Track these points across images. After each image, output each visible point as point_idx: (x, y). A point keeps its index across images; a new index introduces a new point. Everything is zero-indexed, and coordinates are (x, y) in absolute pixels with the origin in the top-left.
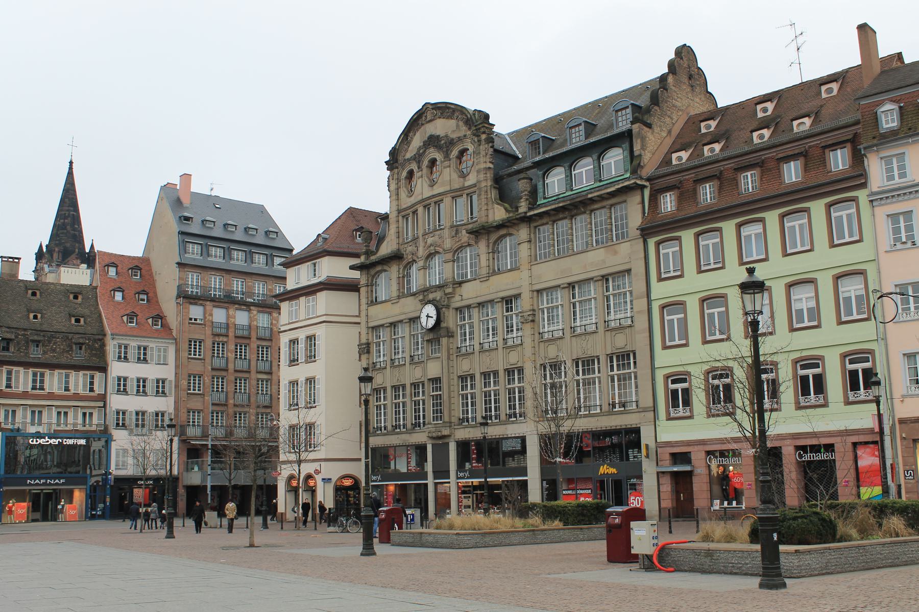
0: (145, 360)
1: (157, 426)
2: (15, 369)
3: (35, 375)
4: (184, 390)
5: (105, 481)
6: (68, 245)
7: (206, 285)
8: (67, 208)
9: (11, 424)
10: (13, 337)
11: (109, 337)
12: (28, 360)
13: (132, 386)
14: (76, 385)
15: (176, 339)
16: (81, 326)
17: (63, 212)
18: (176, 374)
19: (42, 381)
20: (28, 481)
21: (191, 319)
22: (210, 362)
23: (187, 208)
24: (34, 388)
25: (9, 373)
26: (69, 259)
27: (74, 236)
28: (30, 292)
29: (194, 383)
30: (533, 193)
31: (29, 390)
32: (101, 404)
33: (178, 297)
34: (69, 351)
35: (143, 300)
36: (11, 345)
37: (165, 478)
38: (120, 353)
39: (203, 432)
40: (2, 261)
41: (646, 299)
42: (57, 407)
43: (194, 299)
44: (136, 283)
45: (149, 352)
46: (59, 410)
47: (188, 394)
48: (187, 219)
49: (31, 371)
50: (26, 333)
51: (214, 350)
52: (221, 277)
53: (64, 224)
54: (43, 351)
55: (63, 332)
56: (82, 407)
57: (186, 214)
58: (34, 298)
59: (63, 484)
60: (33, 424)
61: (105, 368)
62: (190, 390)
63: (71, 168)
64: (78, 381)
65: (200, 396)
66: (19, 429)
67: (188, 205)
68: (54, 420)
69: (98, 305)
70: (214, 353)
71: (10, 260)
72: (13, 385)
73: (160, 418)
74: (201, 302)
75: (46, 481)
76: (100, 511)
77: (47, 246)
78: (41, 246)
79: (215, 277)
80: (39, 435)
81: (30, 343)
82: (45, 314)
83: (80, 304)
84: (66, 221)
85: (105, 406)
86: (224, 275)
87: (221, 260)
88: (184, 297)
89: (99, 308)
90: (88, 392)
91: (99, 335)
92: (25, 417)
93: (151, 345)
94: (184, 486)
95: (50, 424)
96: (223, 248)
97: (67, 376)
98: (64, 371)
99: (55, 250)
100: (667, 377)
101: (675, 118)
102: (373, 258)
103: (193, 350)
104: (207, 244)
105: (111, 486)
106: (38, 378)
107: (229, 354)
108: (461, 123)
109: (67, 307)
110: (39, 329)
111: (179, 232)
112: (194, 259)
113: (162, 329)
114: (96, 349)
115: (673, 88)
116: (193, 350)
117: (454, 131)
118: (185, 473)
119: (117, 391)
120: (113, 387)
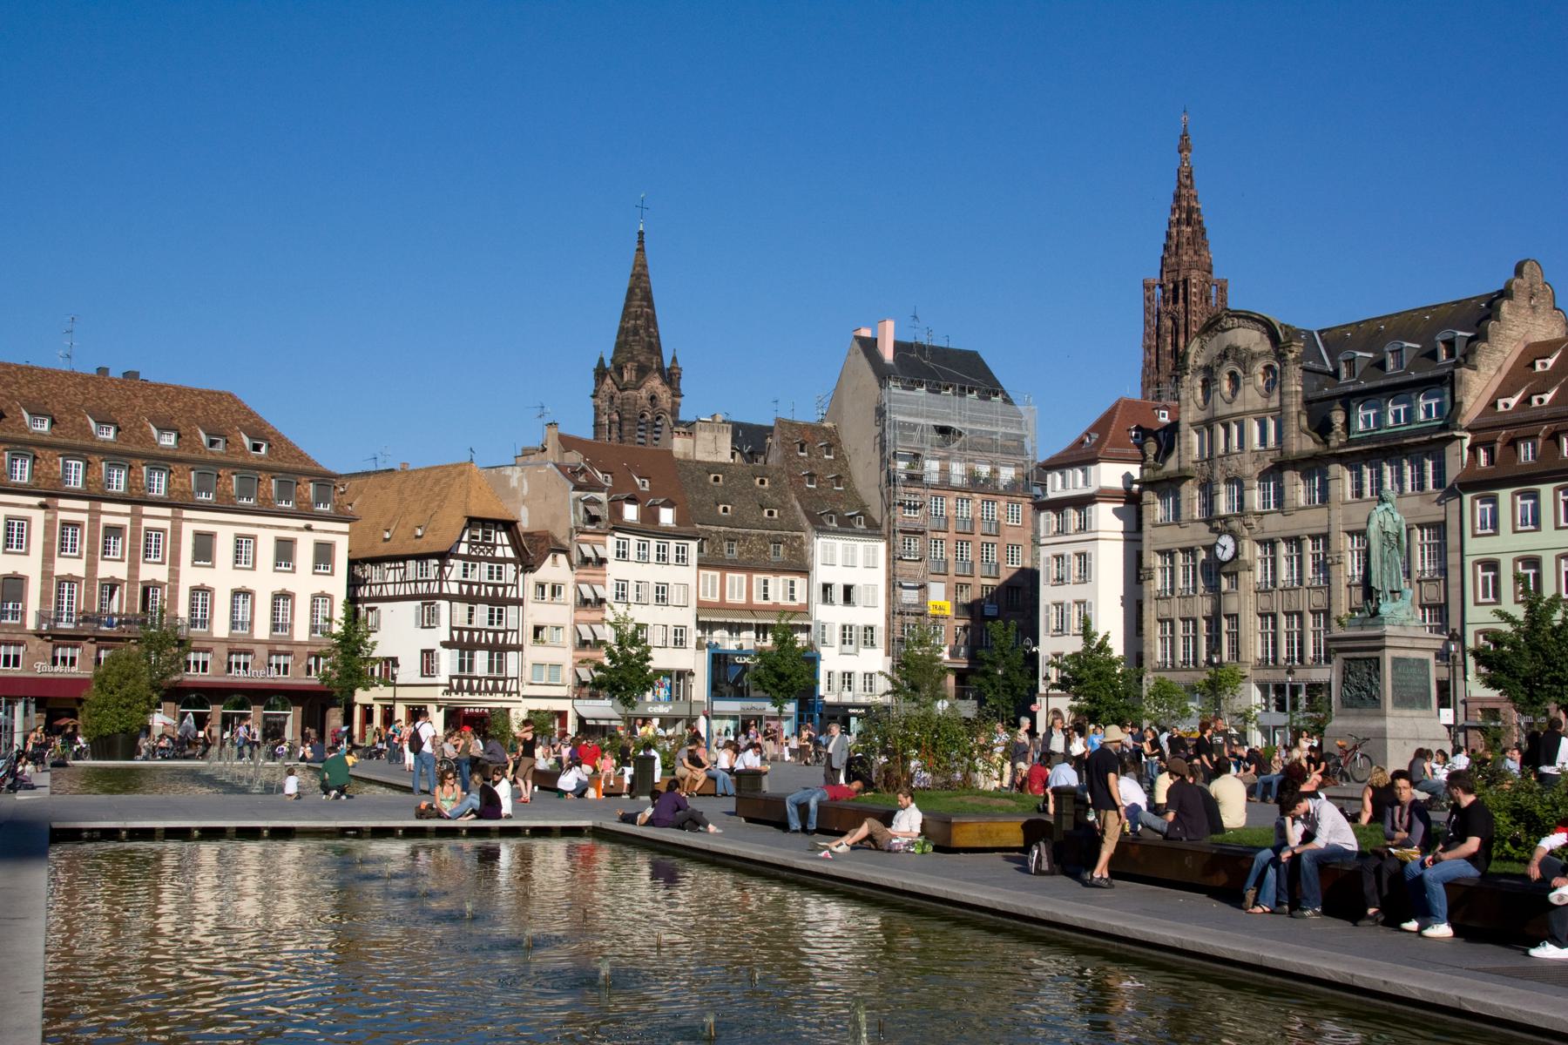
6: (642, 358)
8: (638, 303)
14: (776, 590)
16: (776, 520)
27: (650, 345)
30: (1347, 425)
41: (1458, 554)
64: (778, 587)
77: (612, 361)
78: (601, 360)
98: (762, 577)
100: (1478, 633)
101: (1508, 350)
102: (1159, 474)
107: (950, 555)
108: (1265, 336)
114: (795, 549)
115: (1508, 317)
117: (1256, 344)
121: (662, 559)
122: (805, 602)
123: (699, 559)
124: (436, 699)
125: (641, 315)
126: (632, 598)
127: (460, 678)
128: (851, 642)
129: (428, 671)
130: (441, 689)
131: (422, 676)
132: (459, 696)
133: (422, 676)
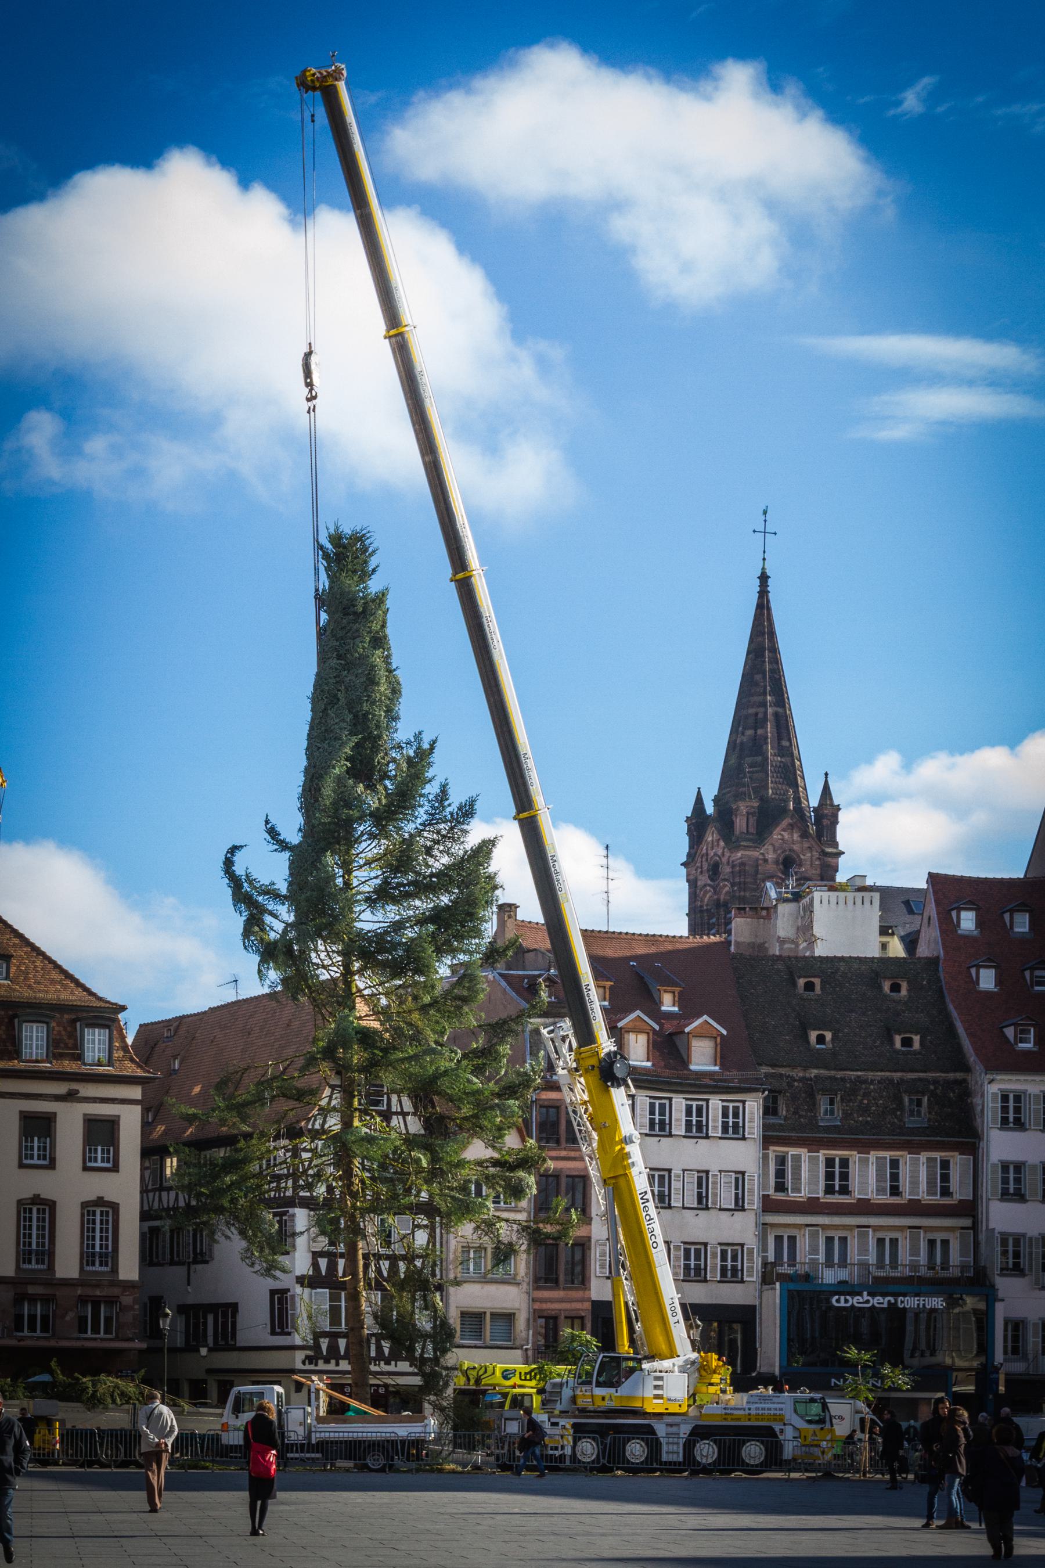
2: (792, 1151)
3: (830, 1162)
9: (789, 1266)
17: (752, 711)
19: (845, 1176)
20: (833, 1380)
24: (829, 1190)
31: (821, 1194)
49: (822, 1155)
50: (807, 1075)
60: (829, 1263)
63: (763, 593)
68: (872, 1258)
80: (845, 1288)
92: (814, 1250)
95: (864, 1265)
99: (737, 809)
121: (697, 1129)
122: (971, 1198)
123: (766, 1127)
124: (293, 1371)
127: (334, 1336)
129: (281, 1326)
130: (300, 1355)
131: (273, 1333)
132: (332, 1366)
133: (273, 1333)
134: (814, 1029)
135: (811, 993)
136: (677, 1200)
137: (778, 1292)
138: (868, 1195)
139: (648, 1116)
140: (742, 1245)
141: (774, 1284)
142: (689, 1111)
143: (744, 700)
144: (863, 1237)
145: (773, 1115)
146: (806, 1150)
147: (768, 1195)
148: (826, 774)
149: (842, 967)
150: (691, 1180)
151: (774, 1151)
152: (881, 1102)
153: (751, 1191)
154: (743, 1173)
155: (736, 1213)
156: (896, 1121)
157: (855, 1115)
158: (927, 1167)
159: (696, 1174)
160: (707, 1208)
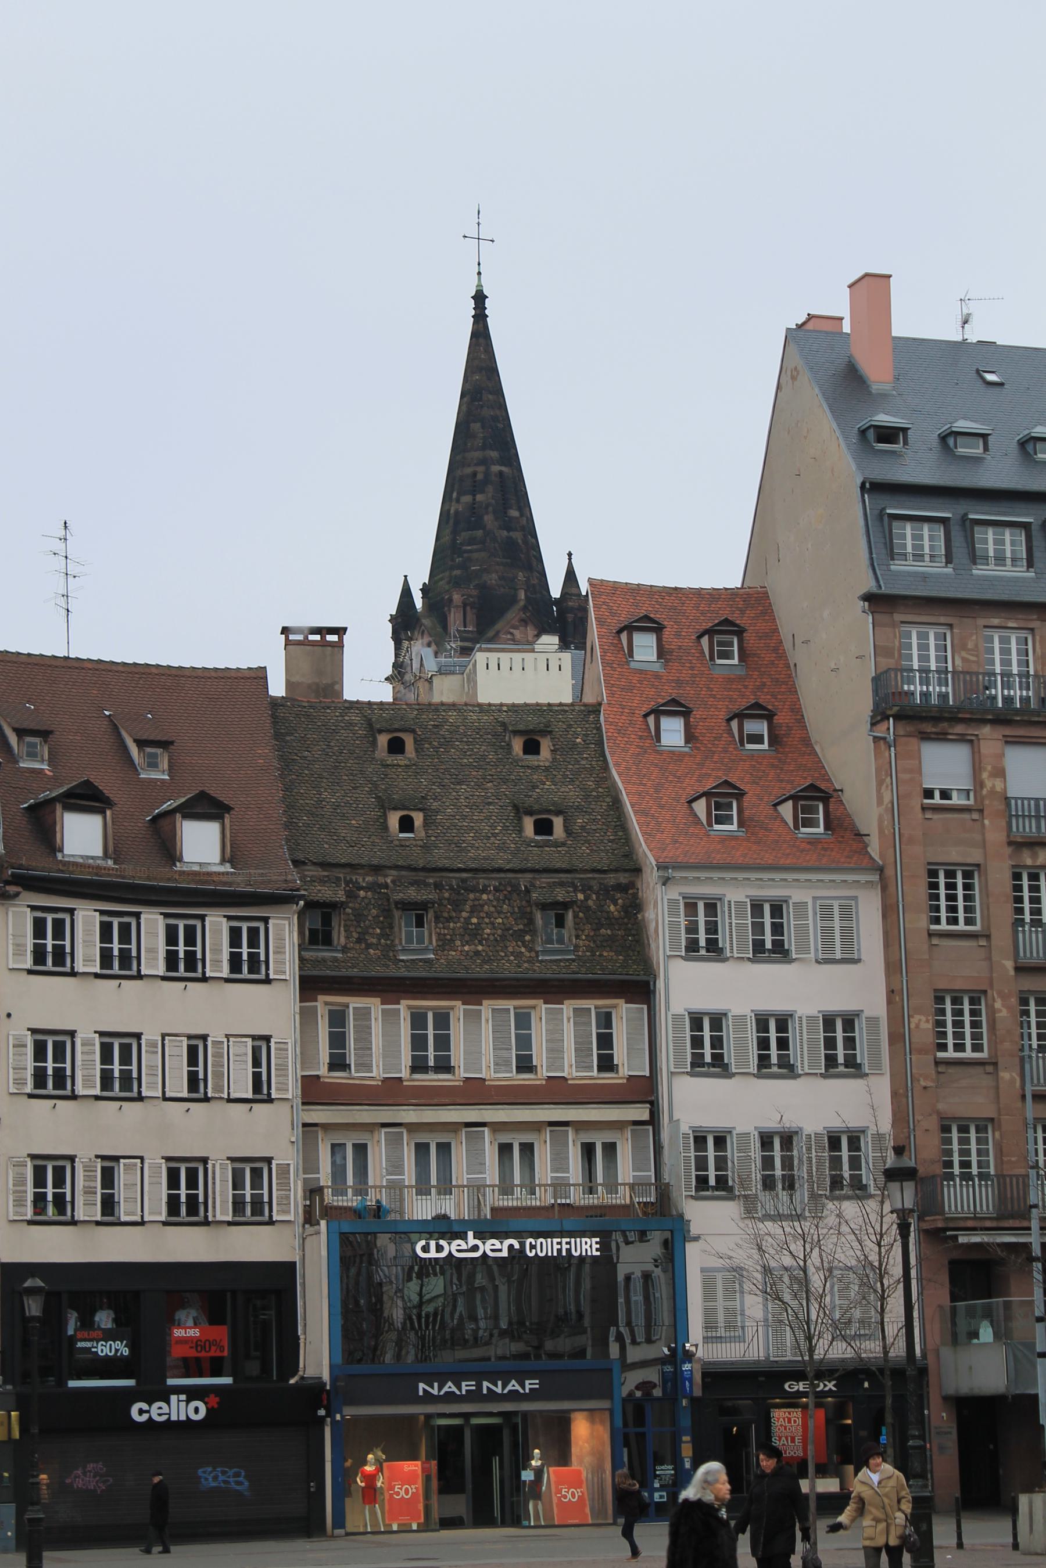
0: (780, 952)
1: (836, 1182)
3: (418, 1020)
4: (920, 1051)
5: (674, 1381)
7: (974, 668)
8: (477, 454)
10: (341, 896)
11: (651, 876)
12: (392, 972)
13: (741, 1043)
14: (555, 1051)
15: (881, 870)
16: (556, 844)
17: (469, 470)
18: (891, 993)
19: (443, 1042)
20: (421, 1386)
21: (929, 793)
22: (1010, 942)
23: (884, 396)
24: (419, 1066)
25: (337, 1018)
26: (498, 626)
28: (383, 740)
29: (958, 1024)
31: (405, 1073)
32: (641, 1113)
33: (879, 716)
34: (524, 932)
35: (757, 739)
36: (335, 923)
37: (881, 1371)
38: (692, 929)
39: (1002, 1199)
40: (288, 642)
42: (497, 1127)
43: (936, 719)
44: (730, 680)
45: (790, 921)
46: (505, 1138)
47: (938, 1063)
48: (888, 435)
49: (404, 1008)
50: (381, 880)
51: (1019, 900)
52: (1023, 634)
53: (473, 507)
54: (441, 937)
55: (500, 870)
56: (580, 1126)
57: (884, 418)
58: (399, 759)
59: (533, 1395)
60: (422, 1188)
61: (647, 983)
62: (943, 1047)
63: (480, 317)
65: (979, 1070)
66: (379, 1206)
67: (887, 387)
68: (491, 1174)
69: (606, 768)
70: (1020, 911)
71: (312, 637)
72: (352, 1060)
73: (845, 1153)
74: (959, 729)
75: (479, 1386)
76: (662, 1487)
77: (425, 590)
78: (406, 592)
79: (1005, 633)
81: (397, 914)
82: (437, 811)
83: (547, 769)
84: (479, 497)
85: (654, 1120)
86: (1035, 624)
87: (1021, 572)
88: (897, 717)
89: (611, 776)
90: (595, 1073)
91: (616, 870)
92: (396, 1166)
93: (797, 895)
94: (946, 1399)
95: (478, 1188)
96: (1026, 526)
97: (523, 1021)
98: (510, 1004)
99: (450, 600)
103: (943, 903)
104: (964, 518)
105: (693, 1400)
106: (431, 1032)
109: (505, 781)
110: (421, 863)
111: (863, 486)
112: (925, 577)
113: (829, 837)
116: (943, 903)
118: (946, 1352)
119: (693, 1065)
120: (679, 1052)
125: (486, 481)
126: (88, 1084)
128: (790, 1184)
134: (395, 809)
135: (400, 757)
136: (152, 1086)
137: (324, 1237)
138: (480, 1071)
139: (98, 945)
140: (269, 1160)
141: (318, 1224)
142: (171, 938)
143: (458, 458)
144: (475, 1141)
145: (323, 944)
146: (378, 1000)
147: (318, 1077)
148: (570, 555)
149: (452, 717)
150: (176, 1051)
151: (326, 1003)
152: (500, 920)
153: (283, 1068)
154: (267, 1039)
155: (255, 1106)
156: (523, 950)
157: (458, 943)
158: (575, 1023)
159: (185, 1042)
160: (206, 1099)
